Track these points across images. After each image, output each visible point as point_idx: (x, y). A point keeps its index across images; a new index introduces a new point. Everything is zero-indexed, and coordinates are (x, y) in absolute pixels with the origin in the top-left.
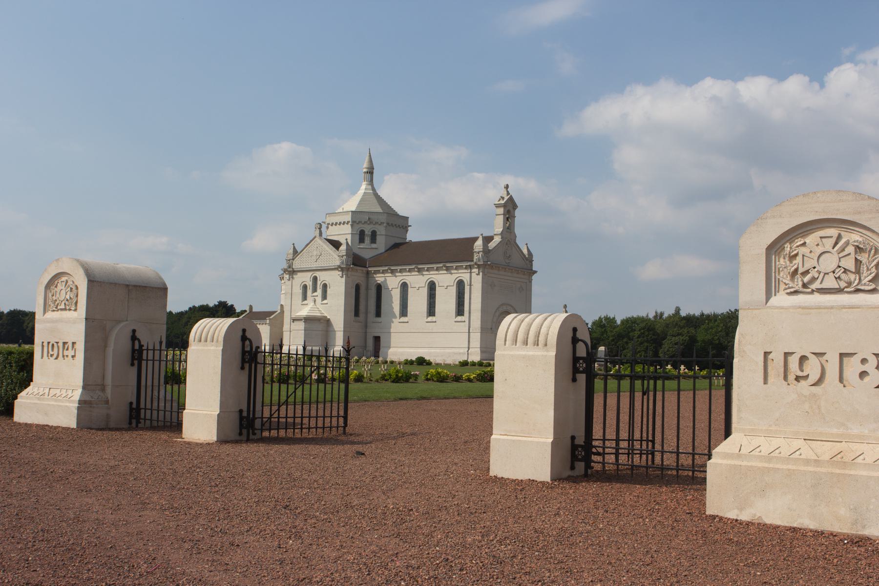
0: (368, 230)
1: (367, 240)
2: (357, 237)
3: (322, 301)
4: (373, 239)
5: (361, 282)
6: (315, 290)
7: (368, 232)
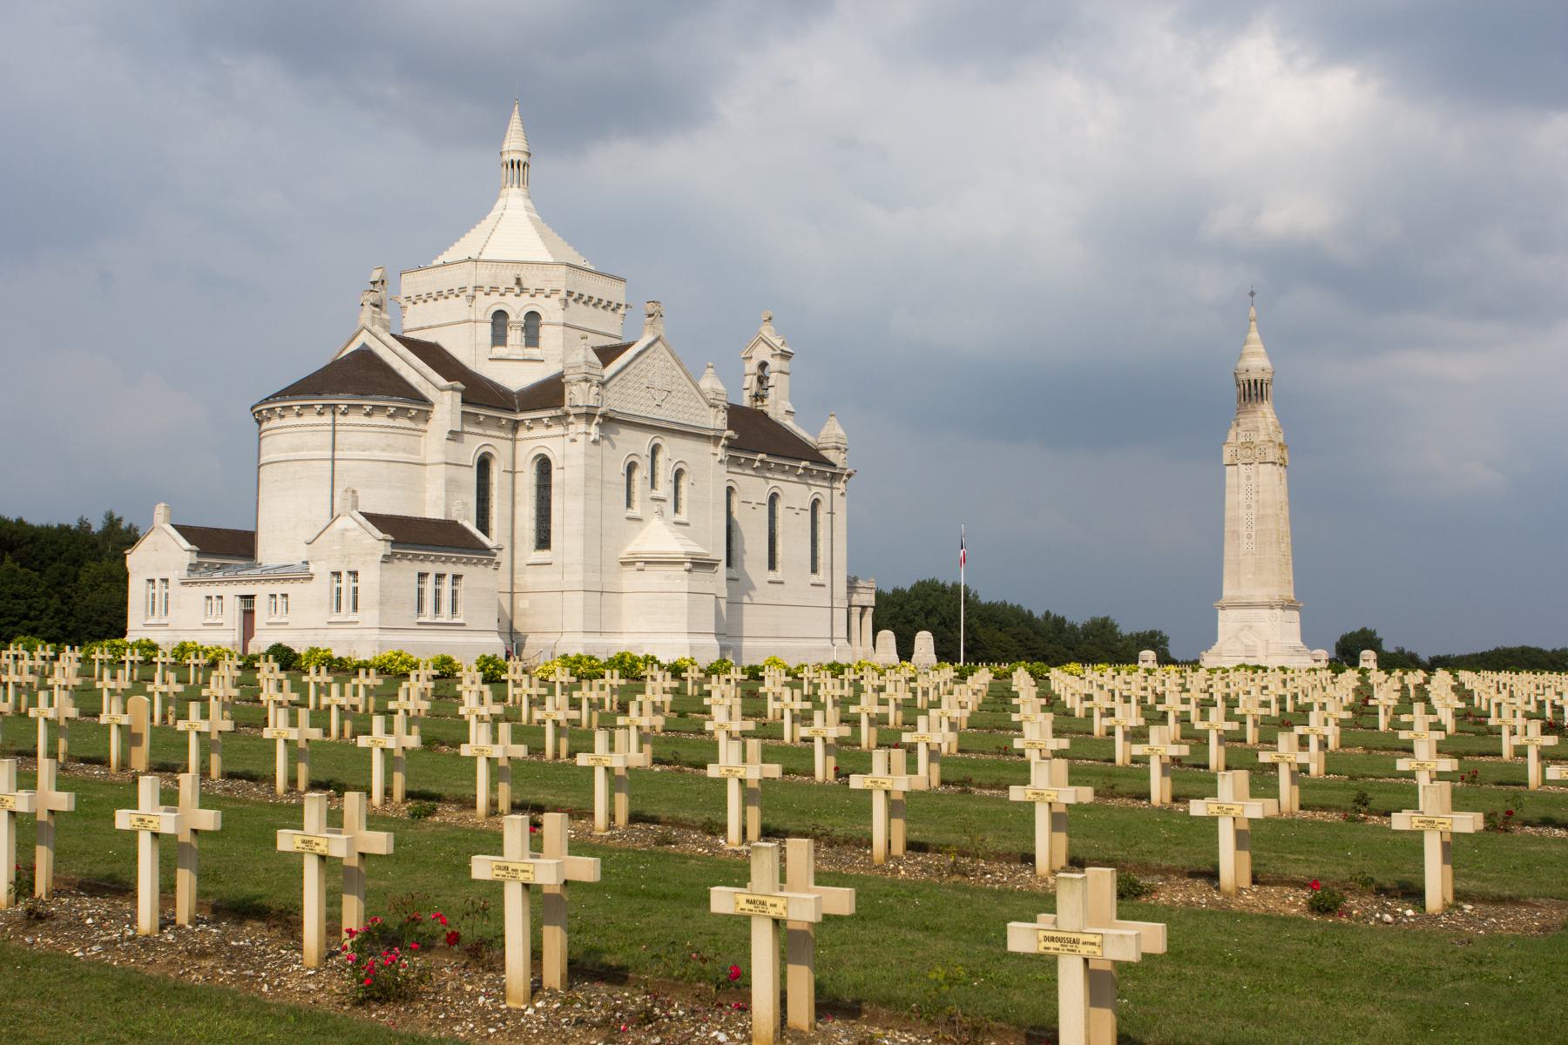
0: (517, 308)
1: (515, 336)
2: (486, 330)
4: (532, 339)
7: (516, 314)
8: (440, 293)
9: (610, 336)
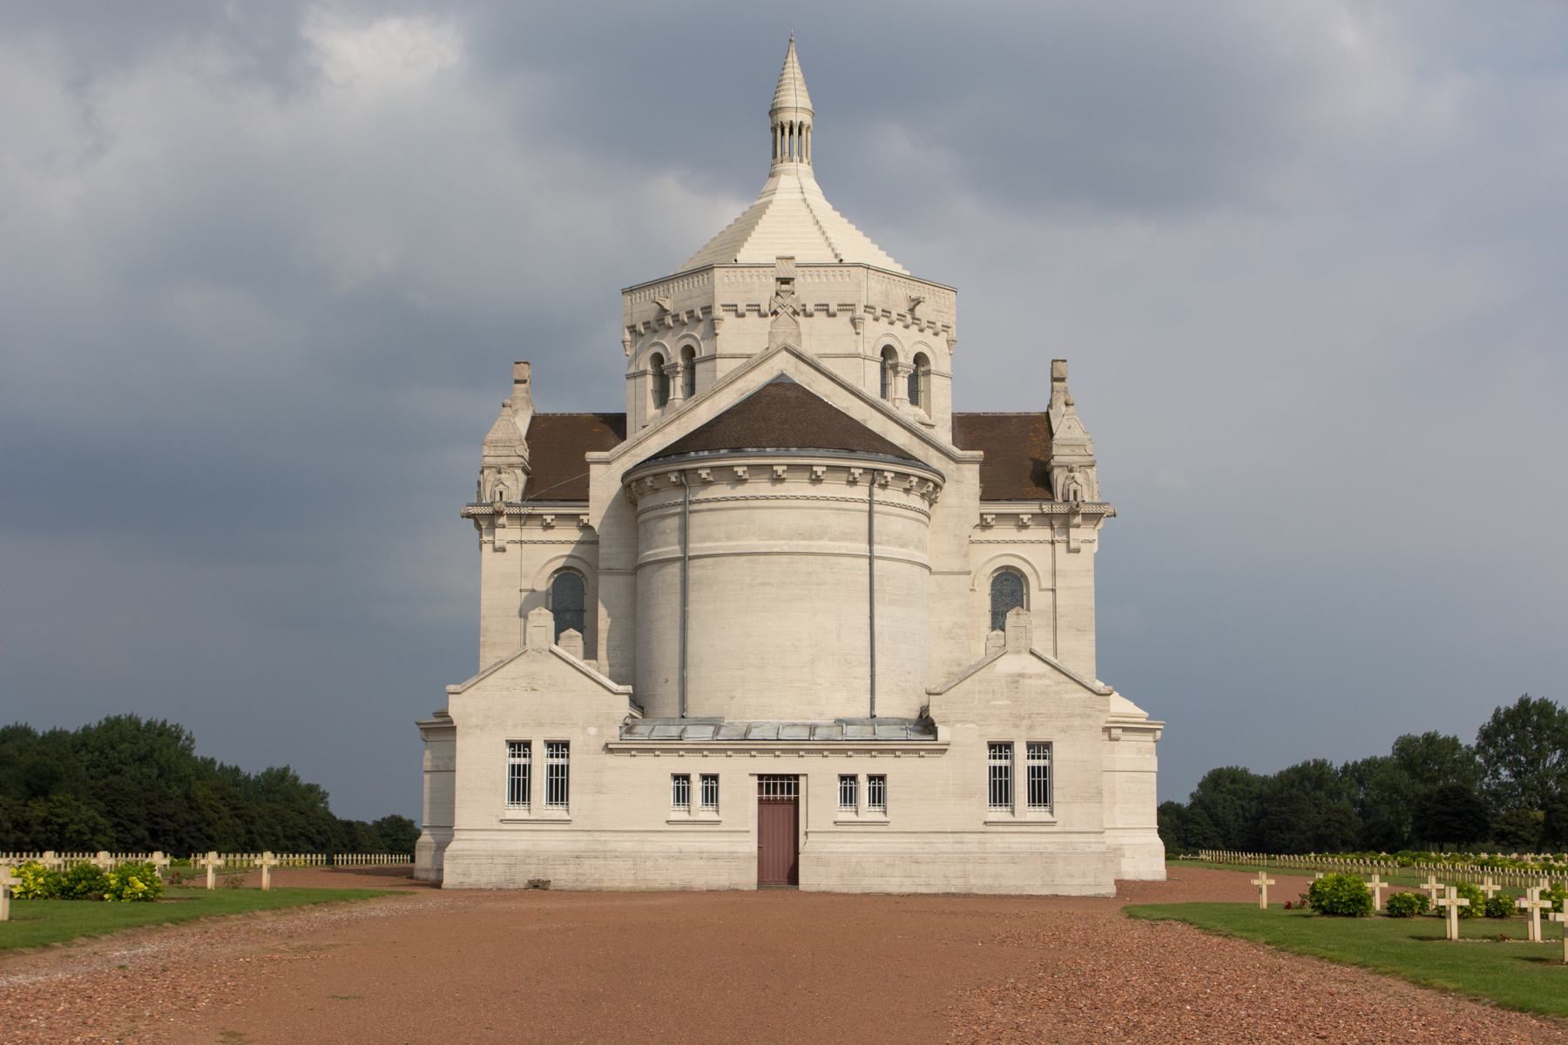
0: (672, 349)
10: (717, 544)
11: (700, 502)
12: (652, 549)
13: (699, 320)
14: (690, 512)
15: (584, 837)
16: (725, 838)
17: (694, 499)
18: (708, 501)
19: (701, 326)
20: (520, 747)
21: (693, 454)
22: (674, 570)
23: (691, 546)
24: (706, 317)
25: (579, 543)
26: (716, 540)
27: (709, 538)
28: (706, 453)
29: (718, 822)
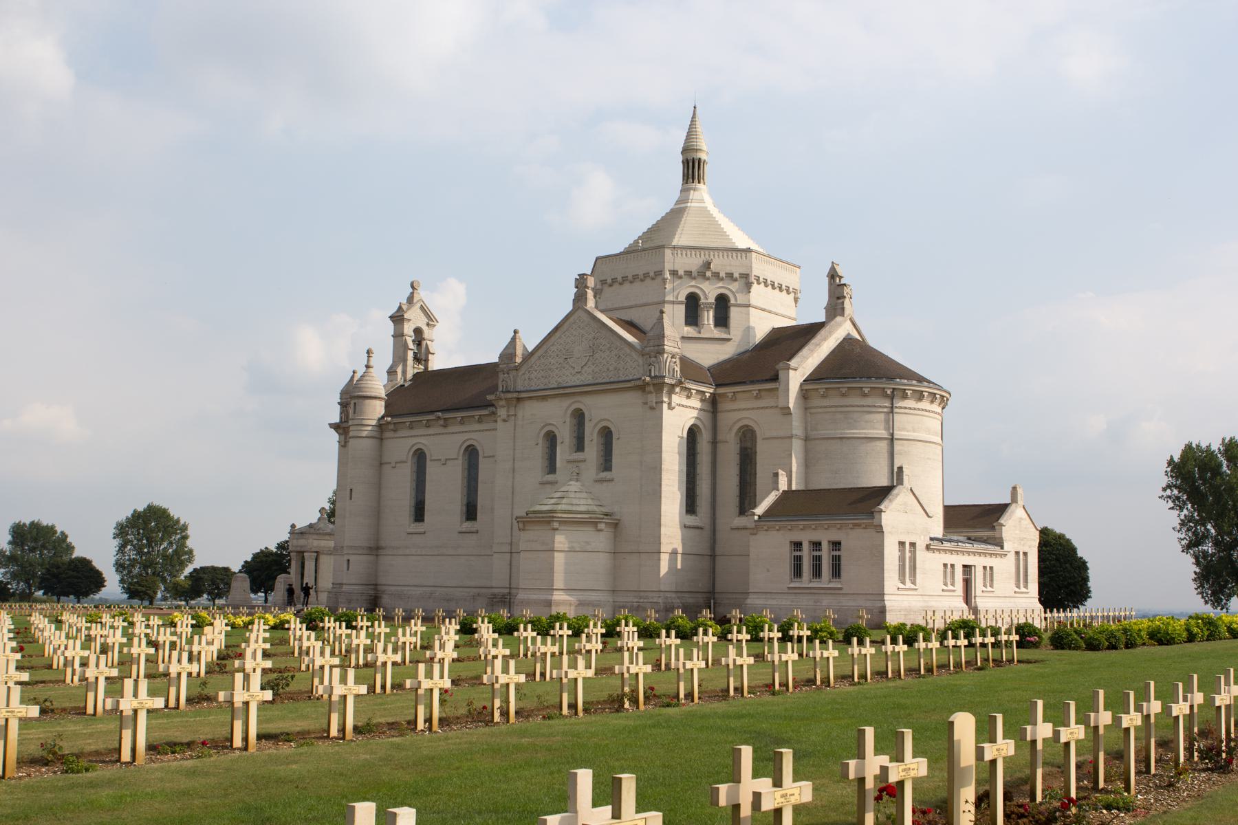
0: (709, 292)
1: (708, 317)
3: (597, 475)
4: (722, 320)
5: (701, 426)
6: (580, 446)
8: (635, 277)
9: (789, 318)
10: (909, 433)
11: (901, 408)
12: (856, 429)
13: (736, 280)
14: (896, 413)
15: (920, 598)
16: (997, 600)
17: (898, 405)
18: (906, 408)
19: (736, 284)
20: (902, 544)
21: (898, 380)
22: (884, 445)
23: (895, 432)
24: (746, 281)
25: (701, 410)
26: (908, 431)
27: (904, 429)
28: (906, 381)
29: (954, 591)
